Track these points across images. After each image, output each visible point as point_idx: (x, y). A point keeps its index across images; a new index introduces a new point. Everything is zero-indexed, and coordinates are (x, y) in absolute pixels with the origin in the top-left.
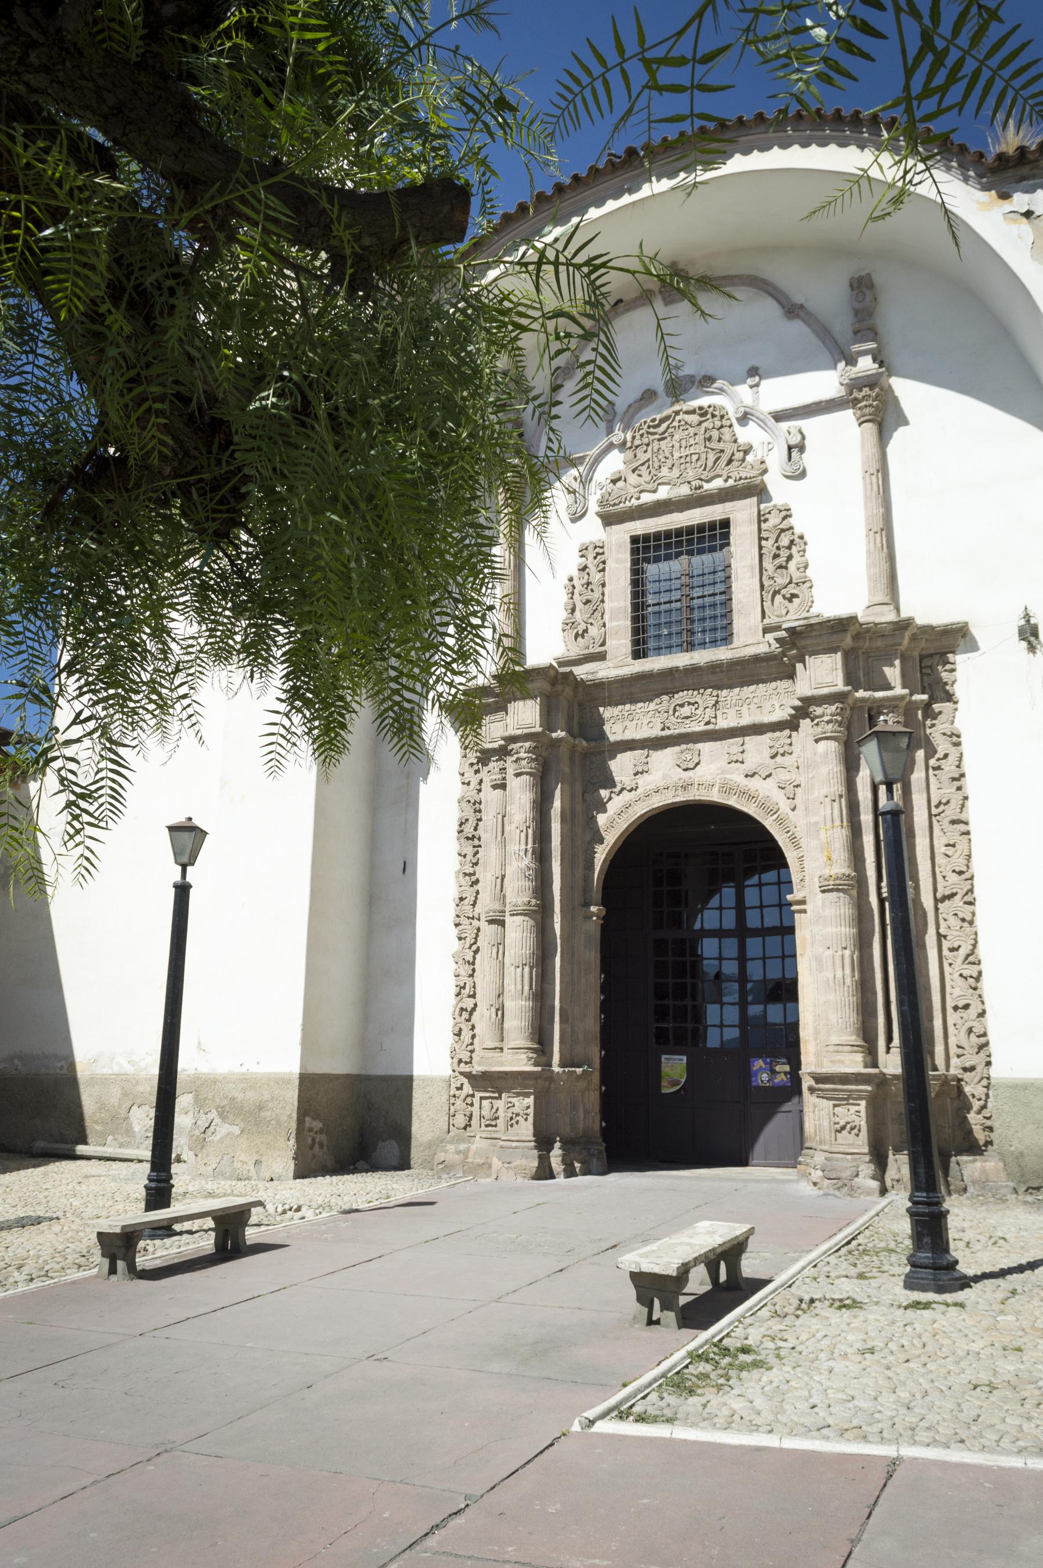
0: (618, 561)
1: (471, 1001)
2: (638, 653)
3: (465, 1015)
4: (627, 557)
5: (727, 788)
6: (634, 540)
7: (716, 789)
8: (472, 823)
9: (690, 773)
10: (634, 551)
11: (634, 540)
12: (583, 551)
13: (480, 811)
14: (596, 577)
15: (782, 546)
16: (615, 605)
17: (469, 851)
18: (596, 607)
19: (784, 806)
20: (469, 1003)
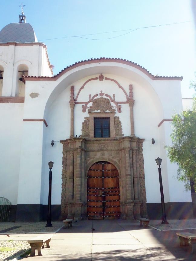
0: (92, 121)
1: (65, 192)
2: (95, 137)
3: (64, 194)
4: (93, 121)
5: (109, 160)
6: (95, 118)
7: (107, 159)
8: (65, 162)
9: (103, 157)
10: (94, 120)
11: (95, 118)
12: (85, 118)
13: (67, 159)
14: (88, 123)
15: (118, 124)
16: (91, 128)
17: (65, 166)
18: (88, 128)
19: (118, 163)
20: (65, 192)
